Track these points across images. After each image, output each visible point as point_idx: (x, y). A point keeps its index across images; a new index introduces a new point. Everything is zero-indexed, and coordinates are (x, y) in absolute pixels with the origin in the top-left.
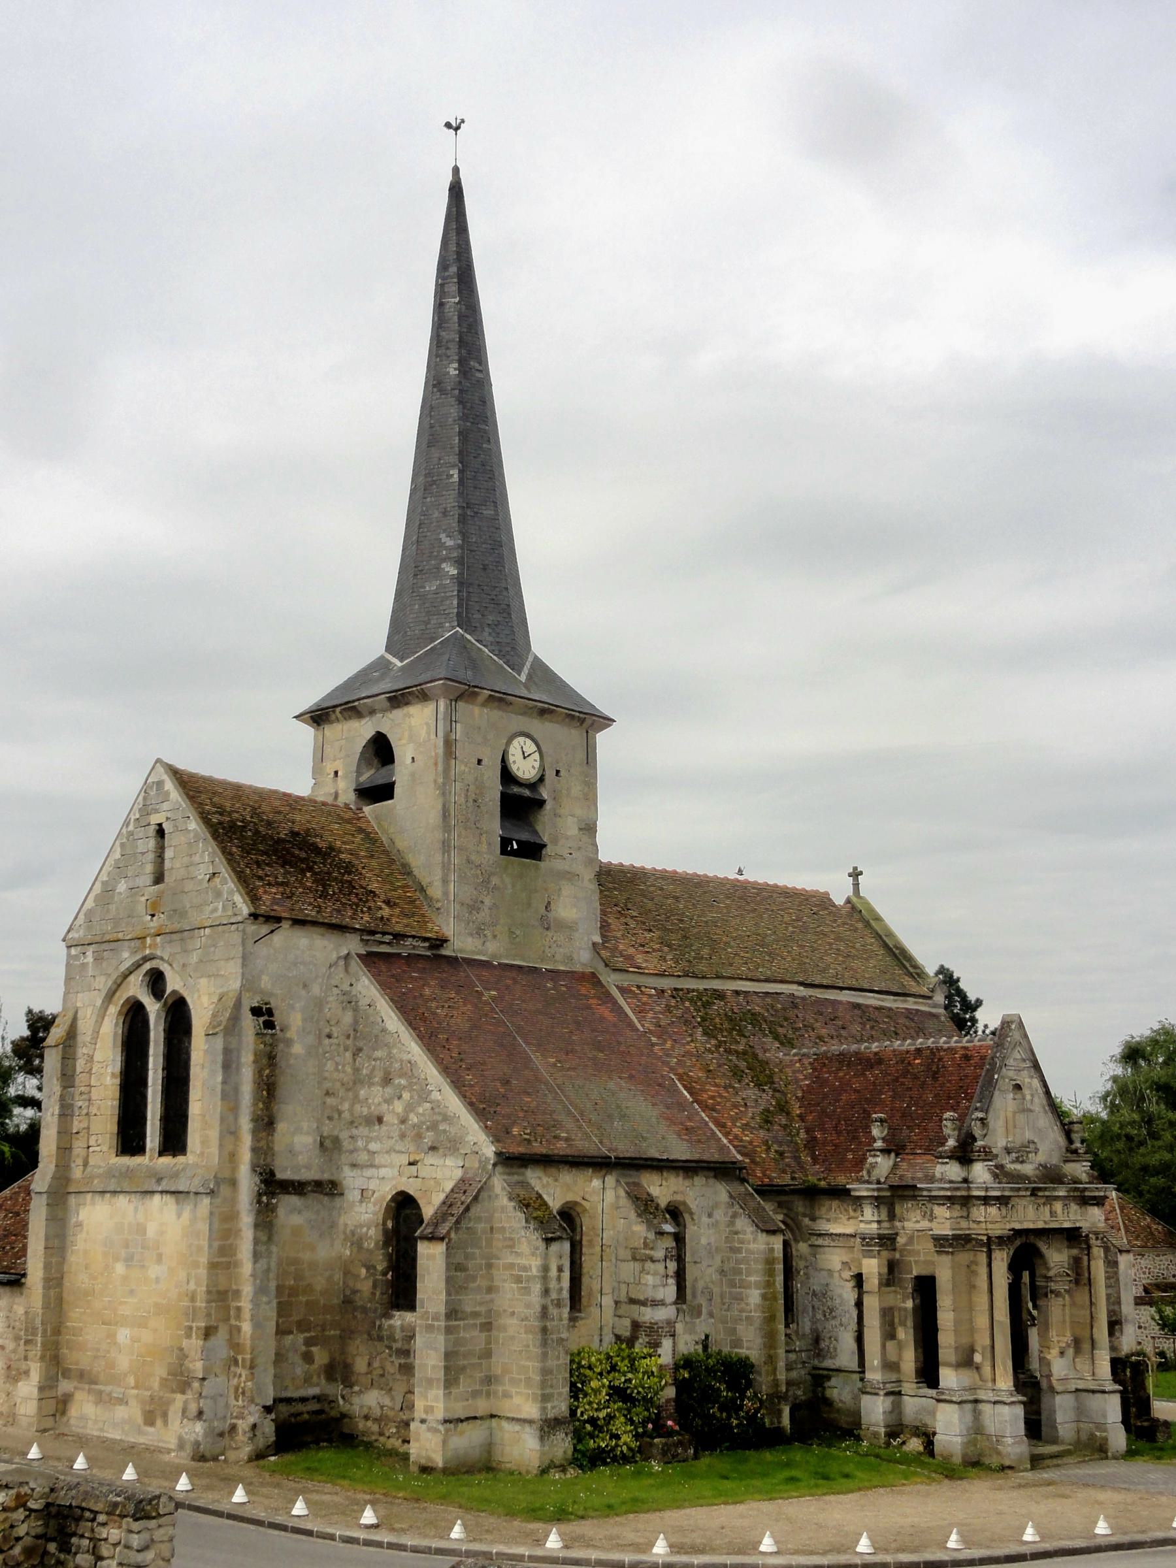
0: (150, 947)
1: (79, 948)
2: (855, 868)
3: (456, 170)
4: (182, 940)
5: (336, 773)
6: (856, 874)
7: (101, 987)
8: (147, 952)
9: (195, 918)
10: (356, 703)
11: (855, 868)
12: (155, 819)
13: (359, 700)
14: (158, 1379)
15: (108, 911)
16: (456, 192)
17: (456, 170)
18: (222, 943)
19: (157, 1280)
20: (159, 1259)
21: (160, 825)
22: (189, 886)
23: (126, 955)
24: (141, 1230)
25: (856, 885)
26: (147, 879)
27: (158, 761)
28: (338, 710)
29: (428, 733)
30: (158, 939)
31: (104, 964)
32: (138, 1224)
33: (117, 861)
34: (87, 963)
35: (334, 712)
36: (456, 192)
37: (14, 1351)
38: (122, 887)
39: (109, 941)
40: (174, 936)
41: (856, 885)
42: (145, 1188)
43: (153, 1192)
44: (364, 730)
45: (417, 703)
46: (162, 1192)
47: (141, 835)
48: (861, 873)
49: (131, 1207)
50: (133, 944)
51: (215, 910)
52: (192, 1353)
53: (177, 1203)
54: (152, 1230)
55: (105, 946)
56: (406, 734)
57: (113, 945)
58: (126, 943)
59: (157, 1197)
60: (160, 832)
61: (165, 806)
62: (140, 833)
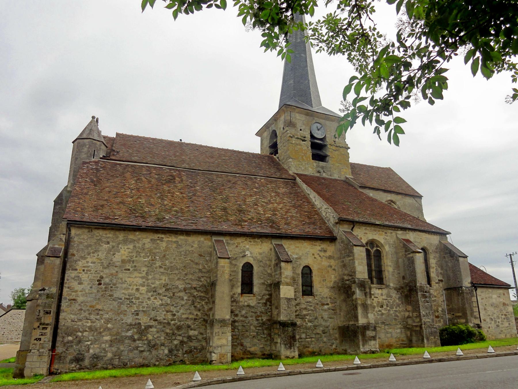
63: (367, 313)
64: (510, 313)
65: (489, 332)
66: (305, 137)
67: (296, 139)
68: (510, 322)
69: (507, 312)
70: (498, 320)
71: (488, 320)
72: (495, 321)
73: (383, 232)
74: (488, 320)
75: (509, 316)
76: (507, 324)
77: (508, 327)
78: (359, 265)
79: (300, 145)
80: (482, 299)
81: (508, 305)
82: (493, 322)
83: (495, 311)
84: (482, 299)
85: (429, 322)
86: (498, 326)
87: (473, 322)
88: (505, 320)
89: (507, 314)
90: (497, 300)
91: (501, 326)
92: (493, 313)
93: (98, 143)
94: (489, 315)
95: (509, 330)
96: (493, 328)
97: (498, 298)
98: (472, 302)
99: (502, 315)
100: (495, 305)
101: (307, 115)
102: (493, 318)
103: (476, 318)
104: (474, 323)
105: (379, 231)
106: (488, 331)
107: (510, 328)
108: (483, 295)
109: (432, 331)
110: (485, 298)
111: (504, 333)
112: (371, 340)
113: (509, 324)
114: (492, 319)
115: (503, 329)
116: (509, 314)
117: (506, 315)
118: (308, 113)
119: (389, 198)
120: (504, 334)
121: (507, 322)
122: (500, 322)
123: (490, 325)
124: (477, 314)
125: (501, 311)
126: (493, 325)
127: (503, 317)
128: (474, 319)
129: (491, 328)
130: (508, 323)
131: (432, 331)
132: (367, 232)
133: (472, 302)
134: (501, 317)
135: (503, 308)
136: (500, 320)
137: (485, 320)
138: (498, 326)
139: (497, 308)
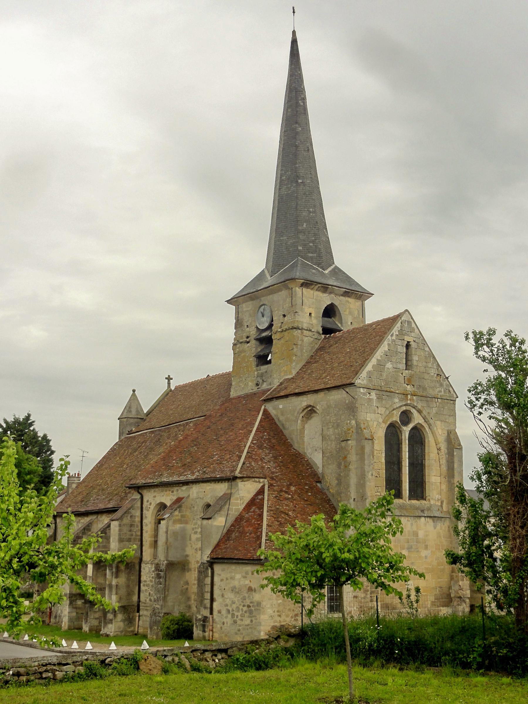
0: (410, 400)
1: (365, 390)
2: (169, 376)
3: (294, 33)
4: (427, 401)
5: (310, 314)
6: (169, 379)
7: (383, 413)
8: (409, 402)
9: (431, 392)
10: (330, 287)
11: (169, 376)
12: (407, 338)
13: (332, 286)
14: (429, 602)
15: (381, 375)
16: (294, 42)
17: (294, 33)
18: (446, 408)
19: (426, 557)
20: (426, 547)
21: (408, 342)
22: (426, 376)
23: (396, 400)
24: (416, 534)
25: (169, 384)
26: (403, 366)
27: (407, 310)
28: (320, 285)
29: (358, 314)
30: (414, 397)
31: (384, 402)
32: (413, 532)
33: (385, 352)
34: (372, 399)
35: (316, 285)
36: (294, 42)
37: (364, 598)
38: (389, 365)
39: (386, 391)
40: (423, 398)
41: (169, 384)
42: (417, 514)
43: (420, 517)
44: (326, 300)
45: (353, 298)
46: (425, 517)
47: (399, 343)
48: (172, 379)
49: (409, 523)
50: (400, 396)
51: (440, 391)
52: (465, 587)
53: (434, 522)
54: (421, 534)
55: (384, 393)
56: (348, 310)
57: (388, 394)
58: (397, 395)
59: (423, 519)
60: (408, 346)
61: (413, 334)
62: (400, 342)
63: (111, 594)
64: (255, 604)
65: (223, 629)
66: (248, 337)
67: (240, 345)
68: (253, 619)
69: (251, 603)
70: (236, 614)
71: (224, 612)
72: (233, 615)
73: (170, 490)
74: (224, 612)
75: (253, 608)
76: (247, 621)
77: (248, 625)
78: (113, 542)
79: (244, 351)
80: (222, 580)
81: (255, 591)
82: (230, 616)
83: (236, 600)
84: (222, 580)
85: (158, 608)
86: (235, 622)
87: (201, 613)
88: (247, 615)
89: (251, 605)
90: (242, 583)
91: (239, 622)
92: (232, 601)
93: (125, 419)
94: (227, 605)
95: (250, 630)
96: (229, 625)
97: (242, 579)
98: (205, 585)
99: (244, 606)
100: (237, 591)
101: (252, 299)
102: (231, 610)
103: (205, 608)
104: (202, 615)
105: (166, 491)
106: (221, 628)
107: (251, 628)
108: (224, 575)
109: (156, 620)
110: (225, 579)
111: (242, 634)
112: (109, 623)
113: (252, 621)
114: (228, 611)
115: (240, 628)
116: (253, 606)
117: (249, 606)
118: (250, 297)
119: (305, 404)
120: (242, 636)
121: (249, 617)
122: (239, 617)
123: (225, 620)
124: (207, 603)
125: (244, 599)
126: (229, 620)
127: (245, 609)
128: (203, 609)
129: (225, 624)
130: (250, 619)
131: (156, 620)
132: (155, 494)
133: (205, 585)
134: (242, 609)
135: (247, 595)
136: (239, 614)
137: (219, 612)
138: (235, 622)
139: (238, 596)
